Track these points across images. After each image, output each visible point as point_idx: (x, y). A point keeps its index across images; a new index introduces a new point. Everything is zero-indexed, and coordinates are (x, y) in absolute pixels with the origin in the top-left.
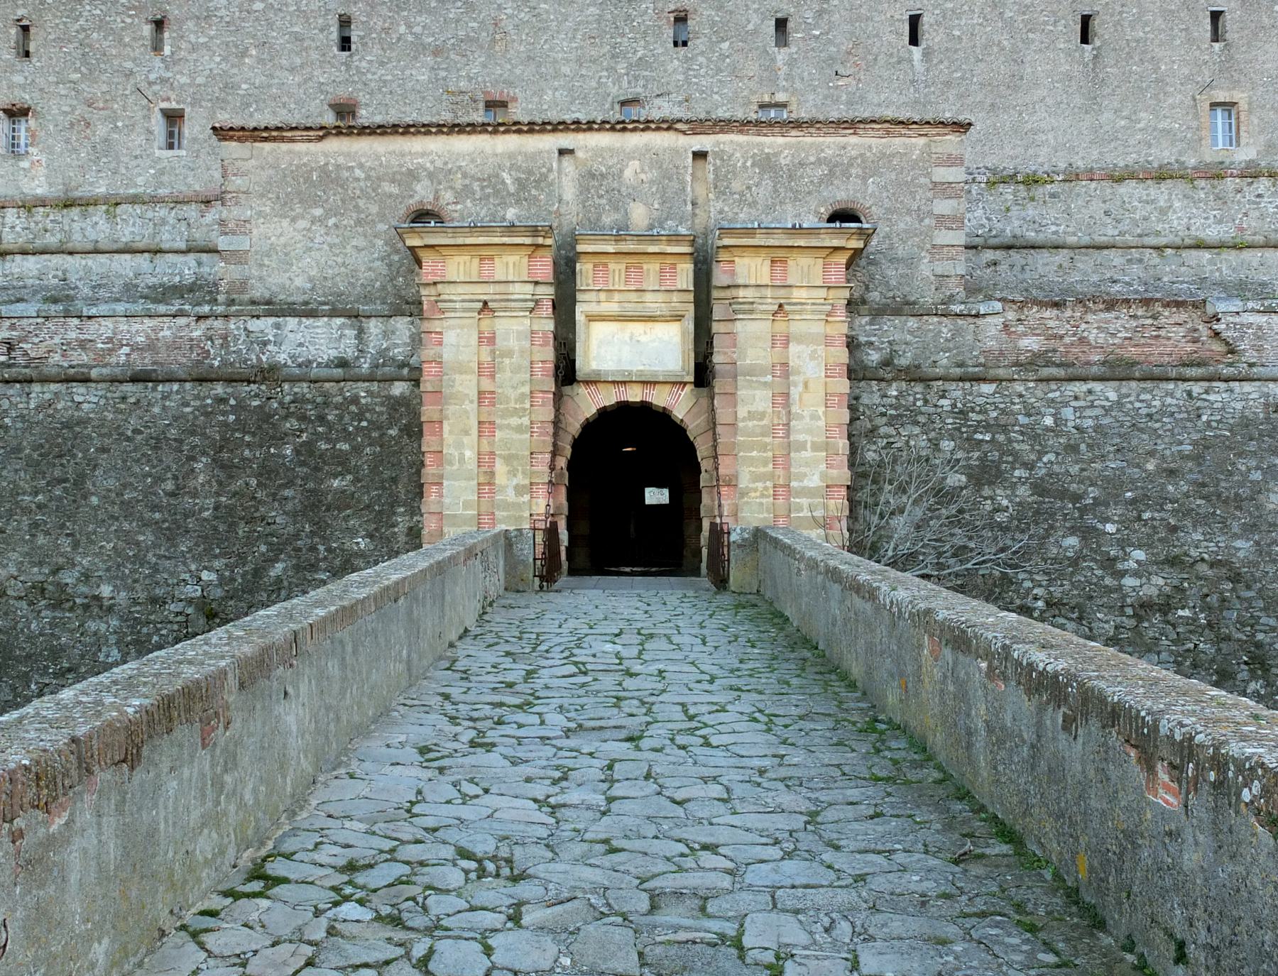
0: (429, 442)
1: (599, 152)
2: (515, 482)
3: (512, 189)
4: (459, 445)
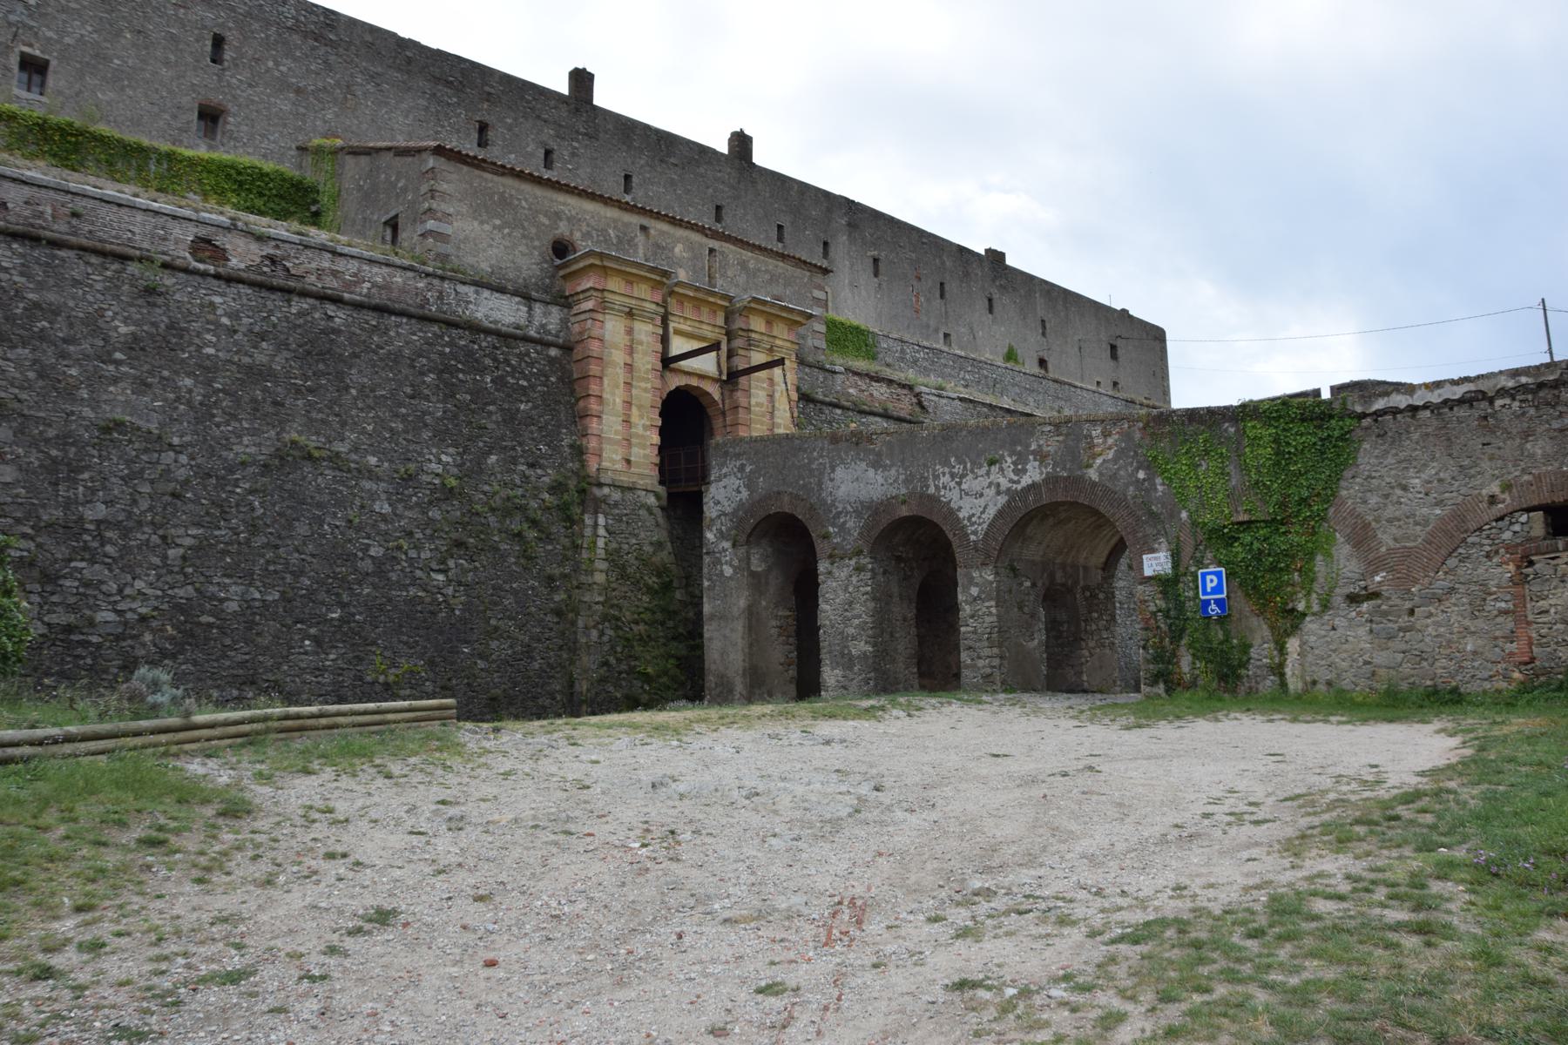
1: (662, 233)
4: (613, 394)
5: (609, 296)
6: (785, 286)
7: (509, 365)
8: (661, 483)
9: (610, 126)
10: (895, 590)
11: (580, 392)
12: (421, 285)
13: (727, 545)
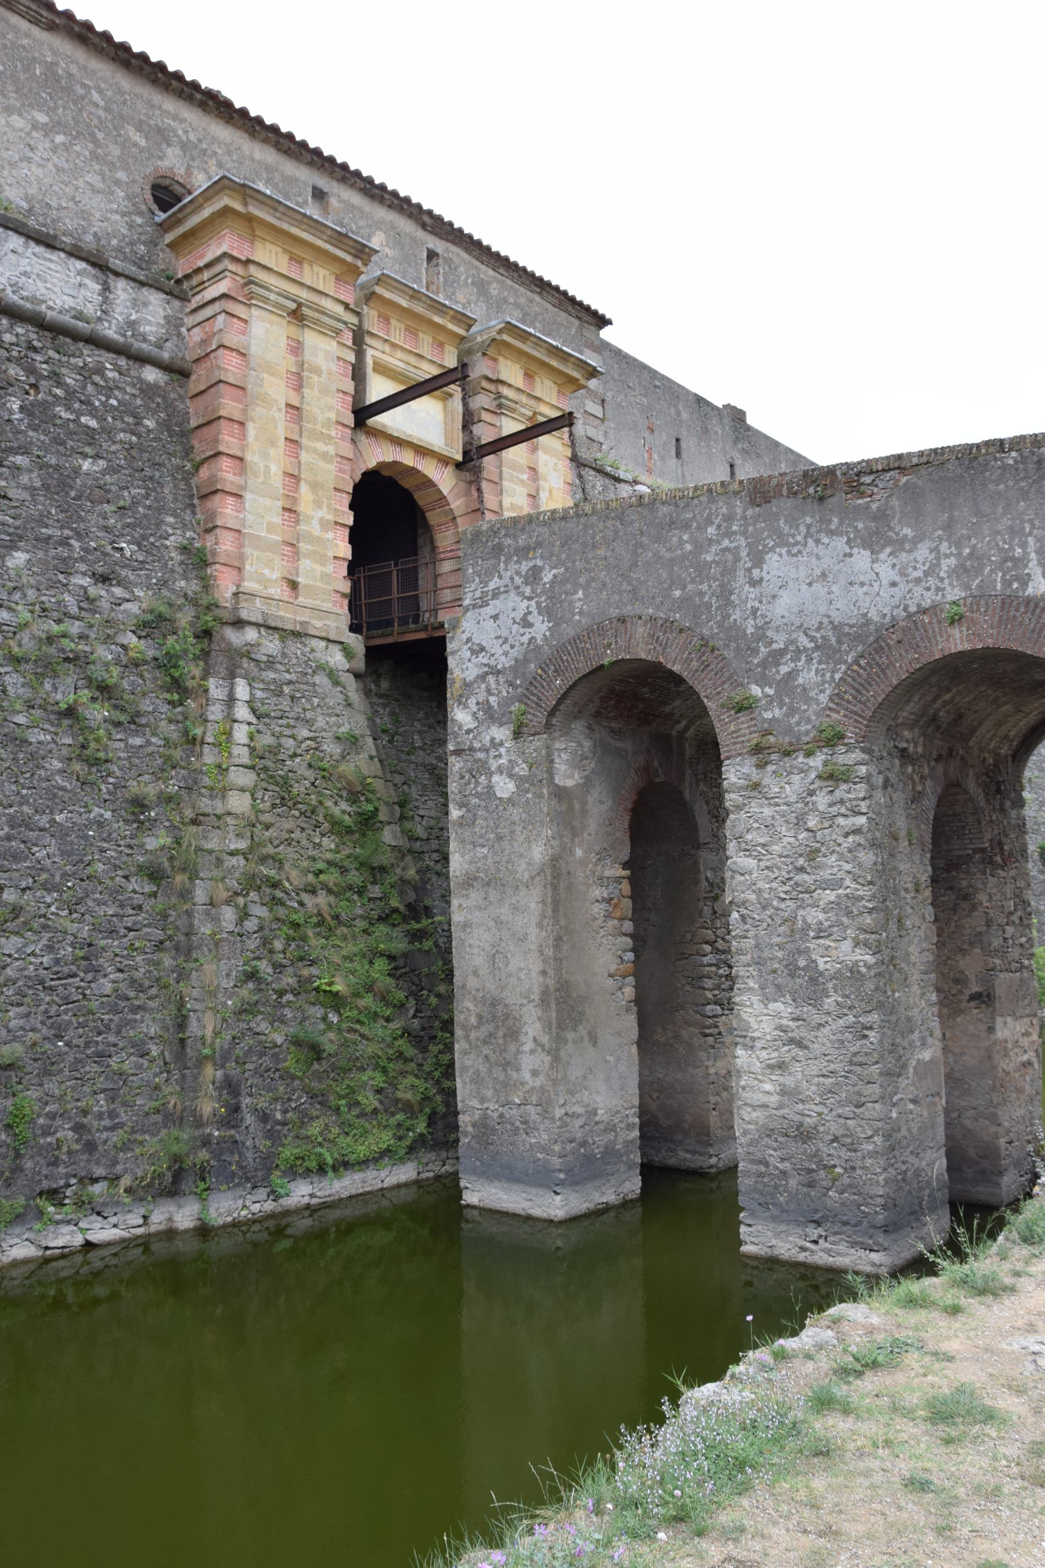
2: (320, 514)
4: (265, 456)
7: (59, 384)
8: (354, 628)
10: (901, 824)
11: (200, 447)
13: (501, 733)
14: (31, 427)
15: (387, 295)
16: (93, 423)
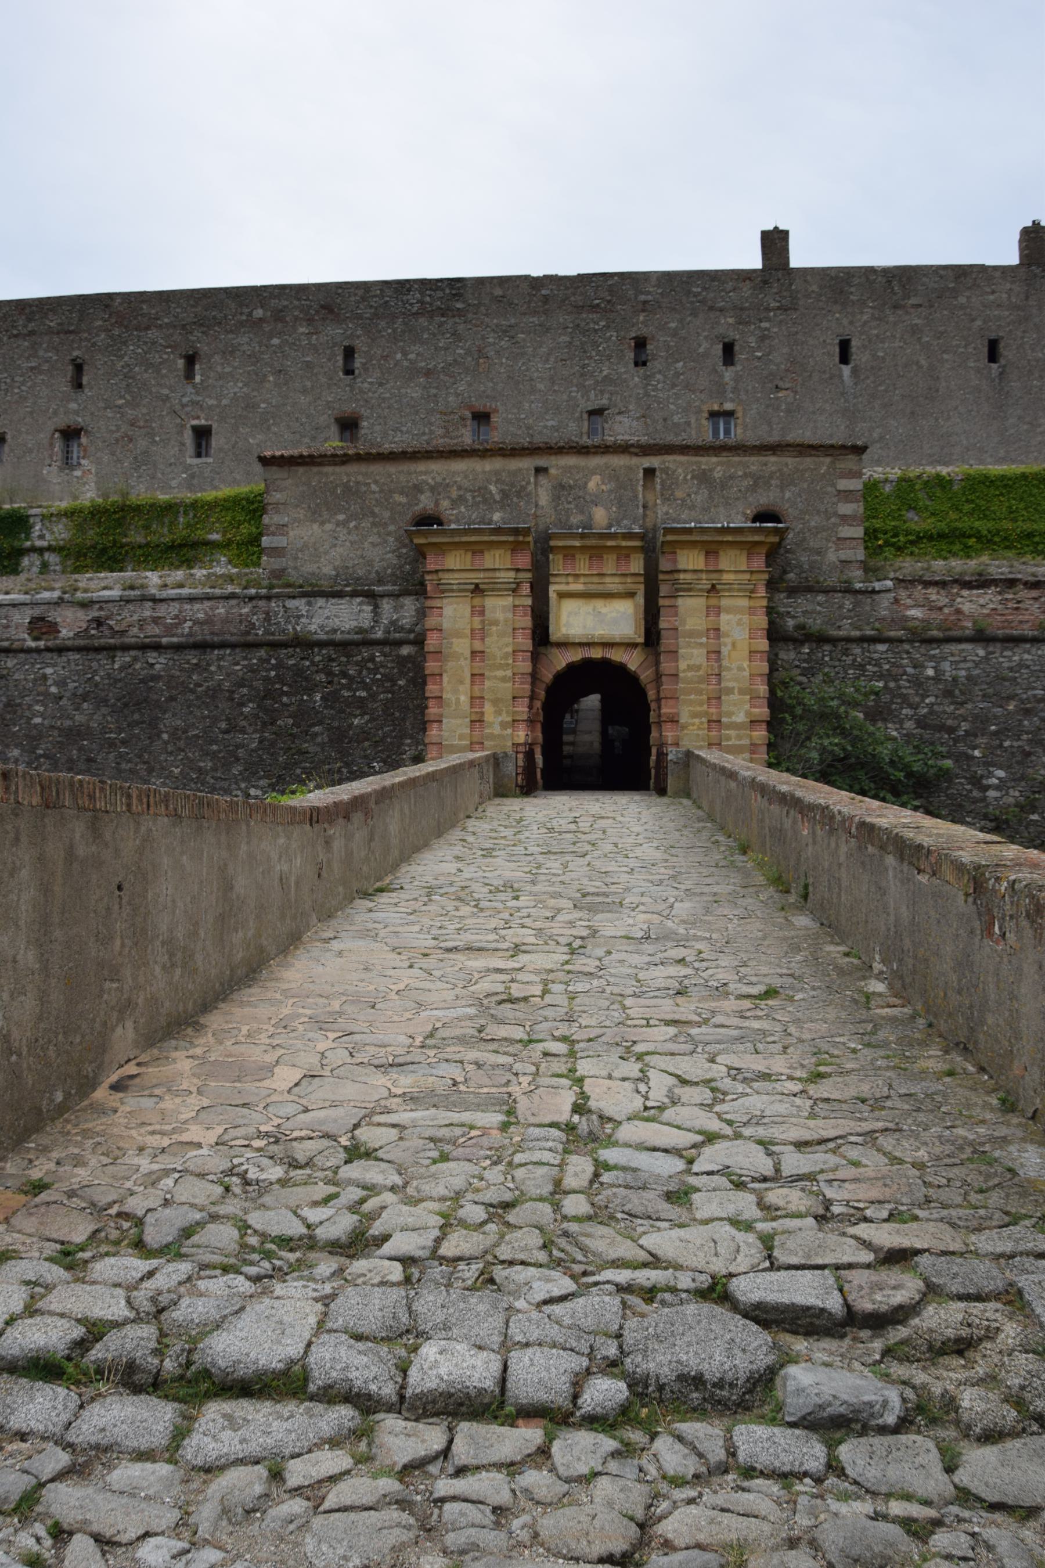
0: (431, 689)
1: (568, 469)
2: (500, 719)
3: (498, 497)
4: (456, 691)
5: (446, 578)
6: (782, 488)
9: (815, 288)
12: (245, 610)
14: (325, 708)
15: (560, 543)
16: (364, 694)
